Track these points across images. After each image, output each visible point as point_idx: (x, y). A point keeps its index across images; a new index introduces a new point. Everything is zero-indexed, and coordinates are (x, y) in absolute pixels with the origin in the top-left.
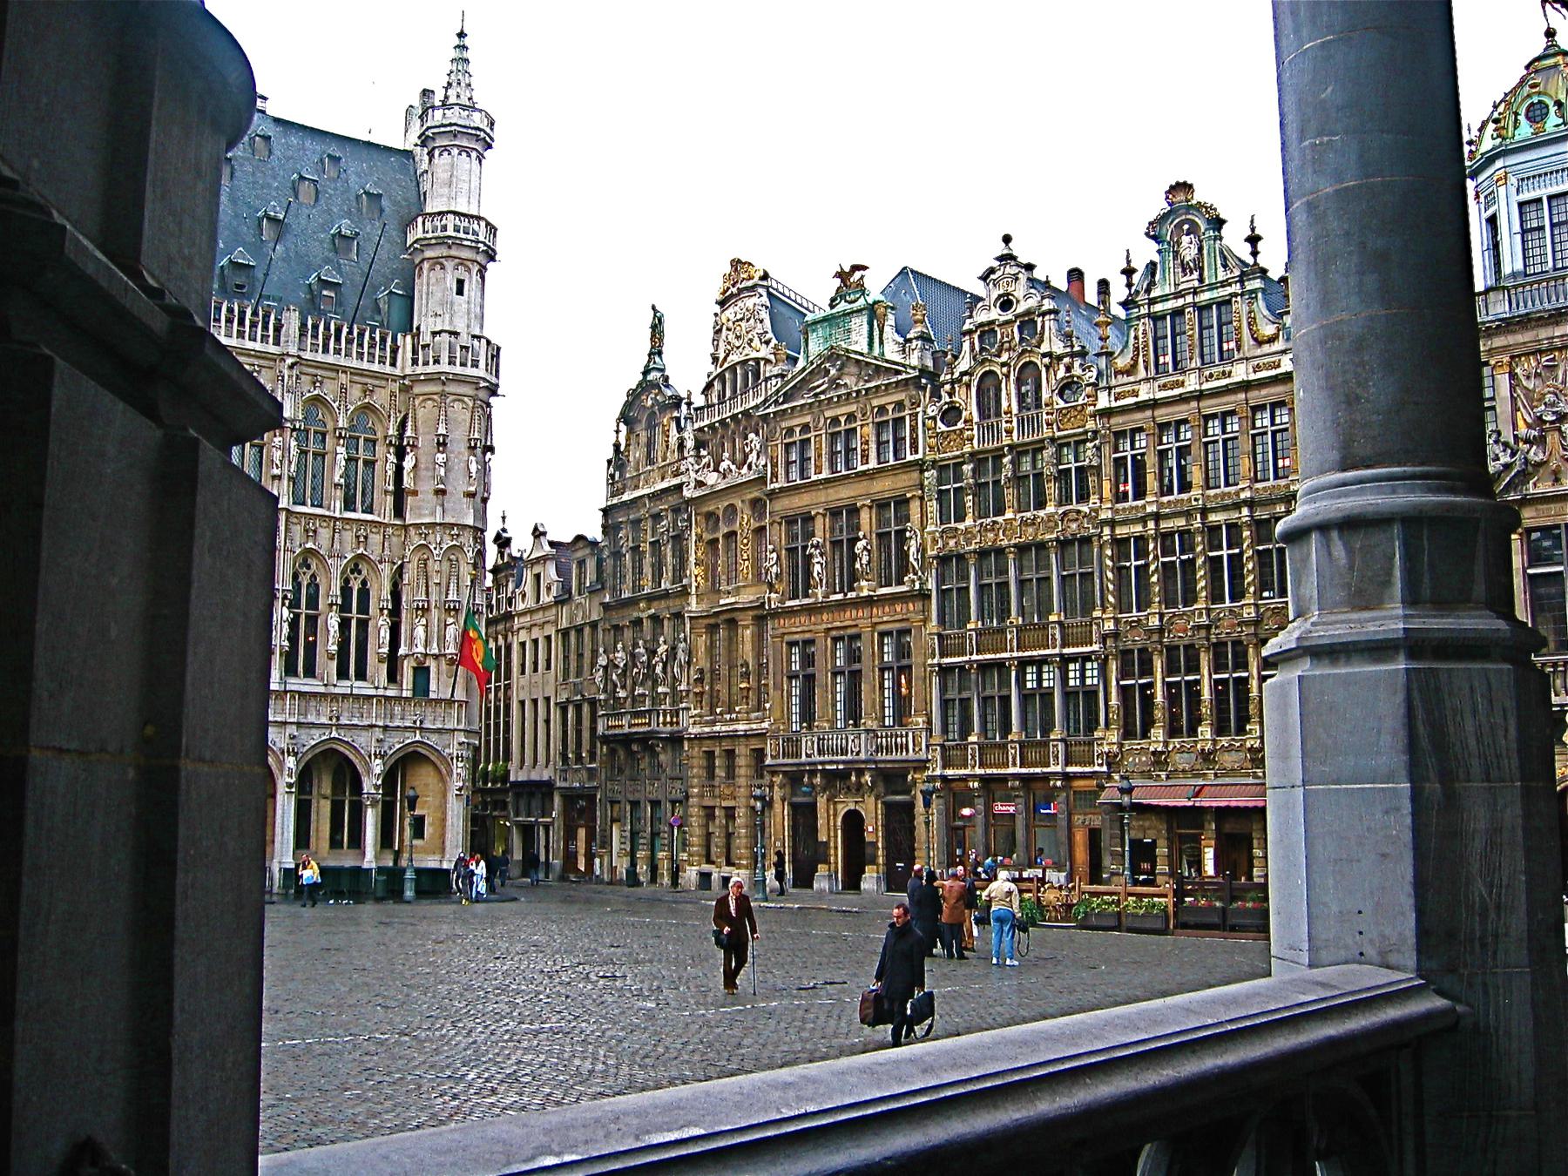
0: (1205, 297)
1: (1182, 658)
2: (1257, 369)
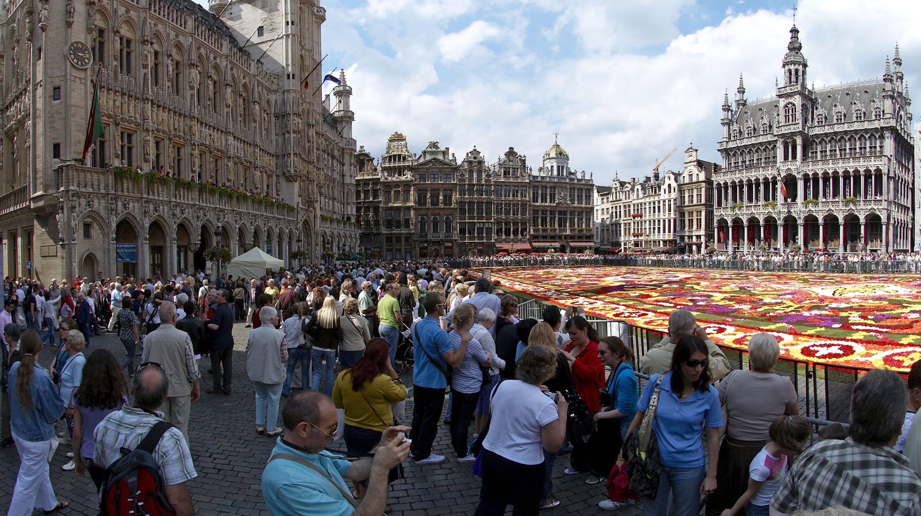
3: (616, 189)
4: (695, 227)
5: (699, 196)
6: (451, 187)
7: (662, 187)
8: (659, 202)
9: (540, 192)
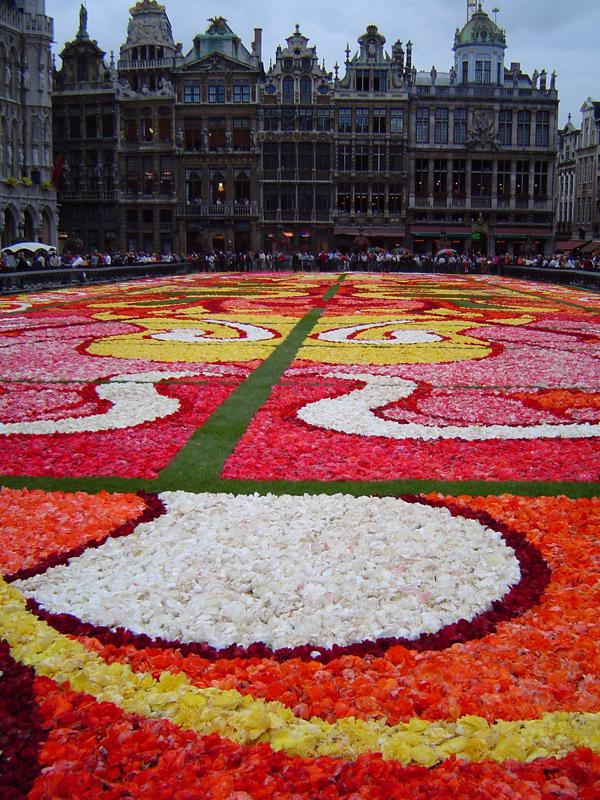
0: (377, 68)
1: (362, 187)
2: (394, 96)
6: (248, 112)
9: (432, 120)
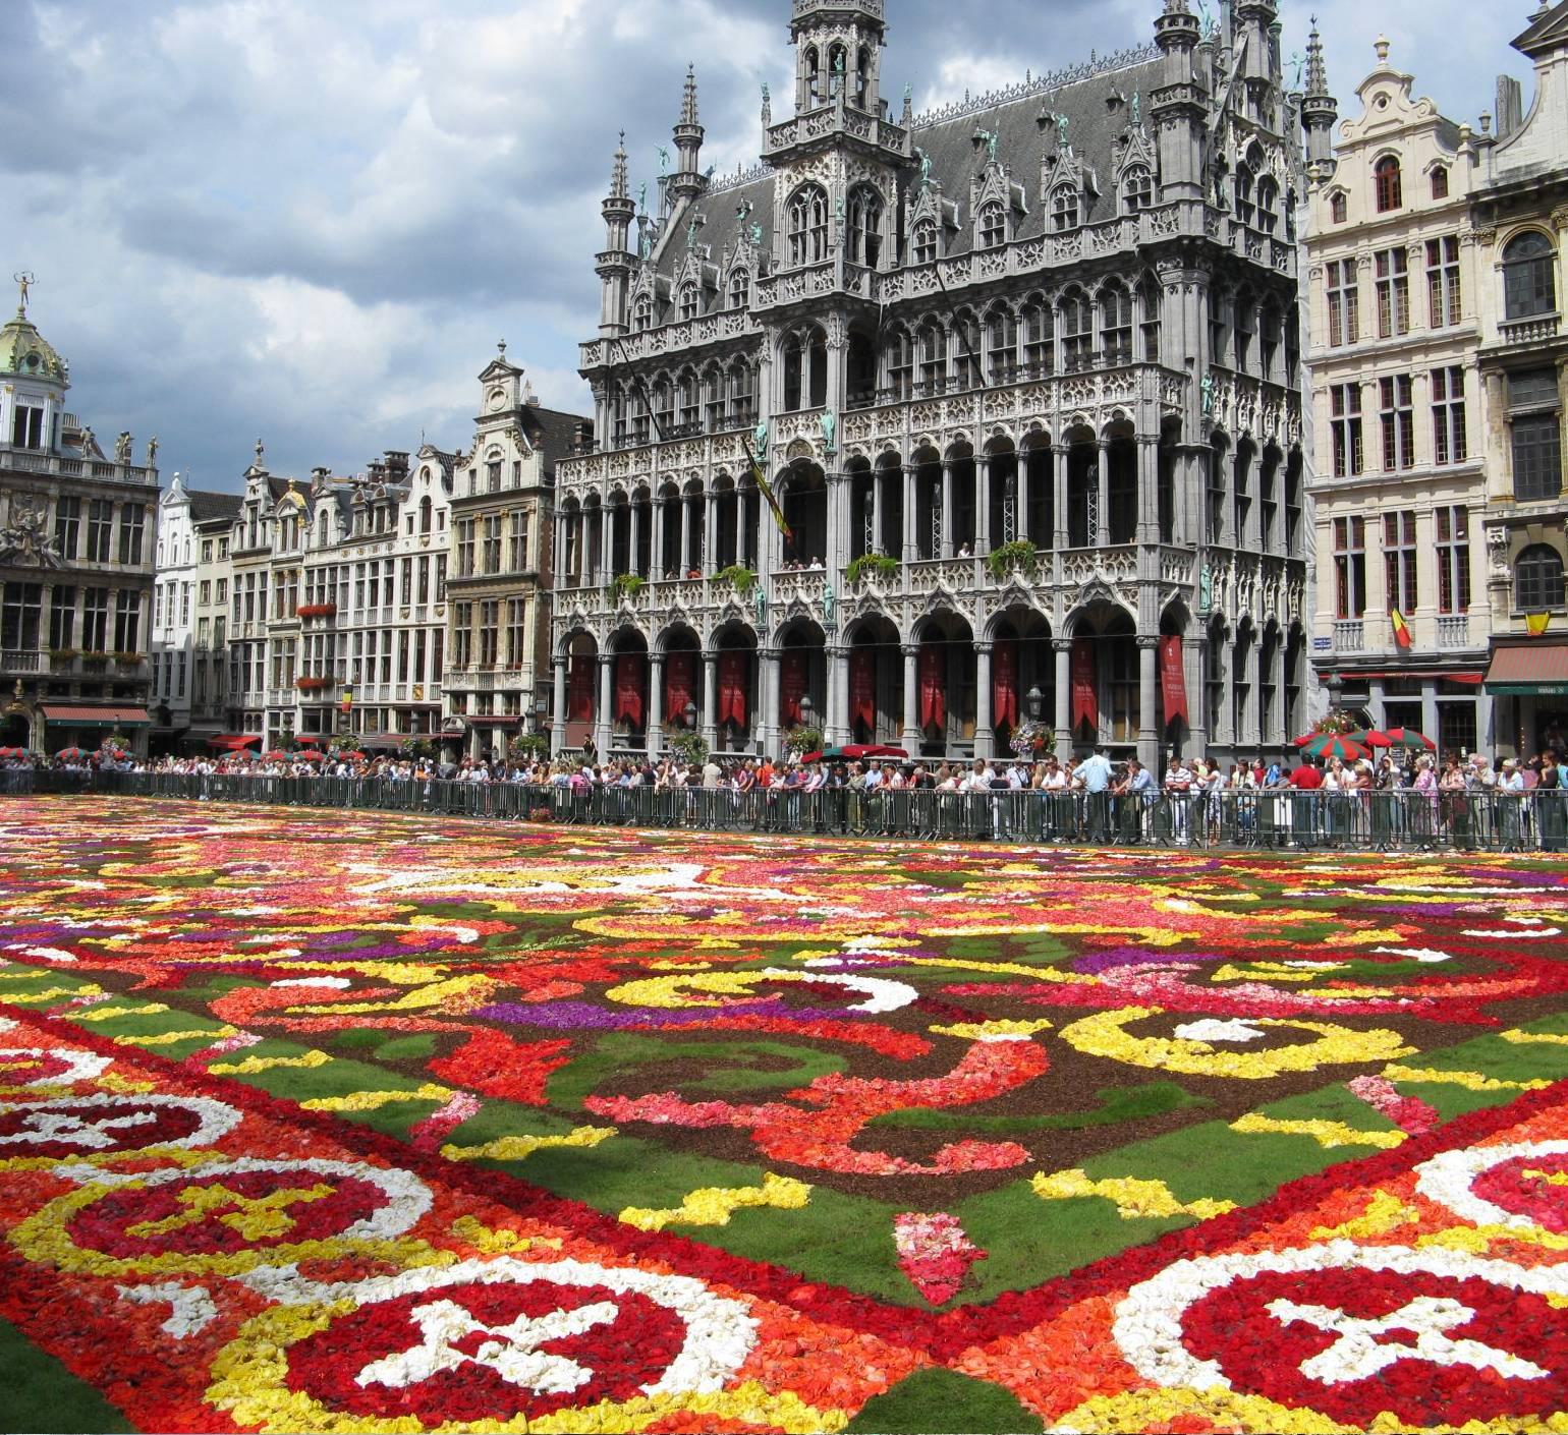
3: (253, 505)
4: (502, 659)
5: (519, 542)
7: (404, 509)
8: (390, 563)
